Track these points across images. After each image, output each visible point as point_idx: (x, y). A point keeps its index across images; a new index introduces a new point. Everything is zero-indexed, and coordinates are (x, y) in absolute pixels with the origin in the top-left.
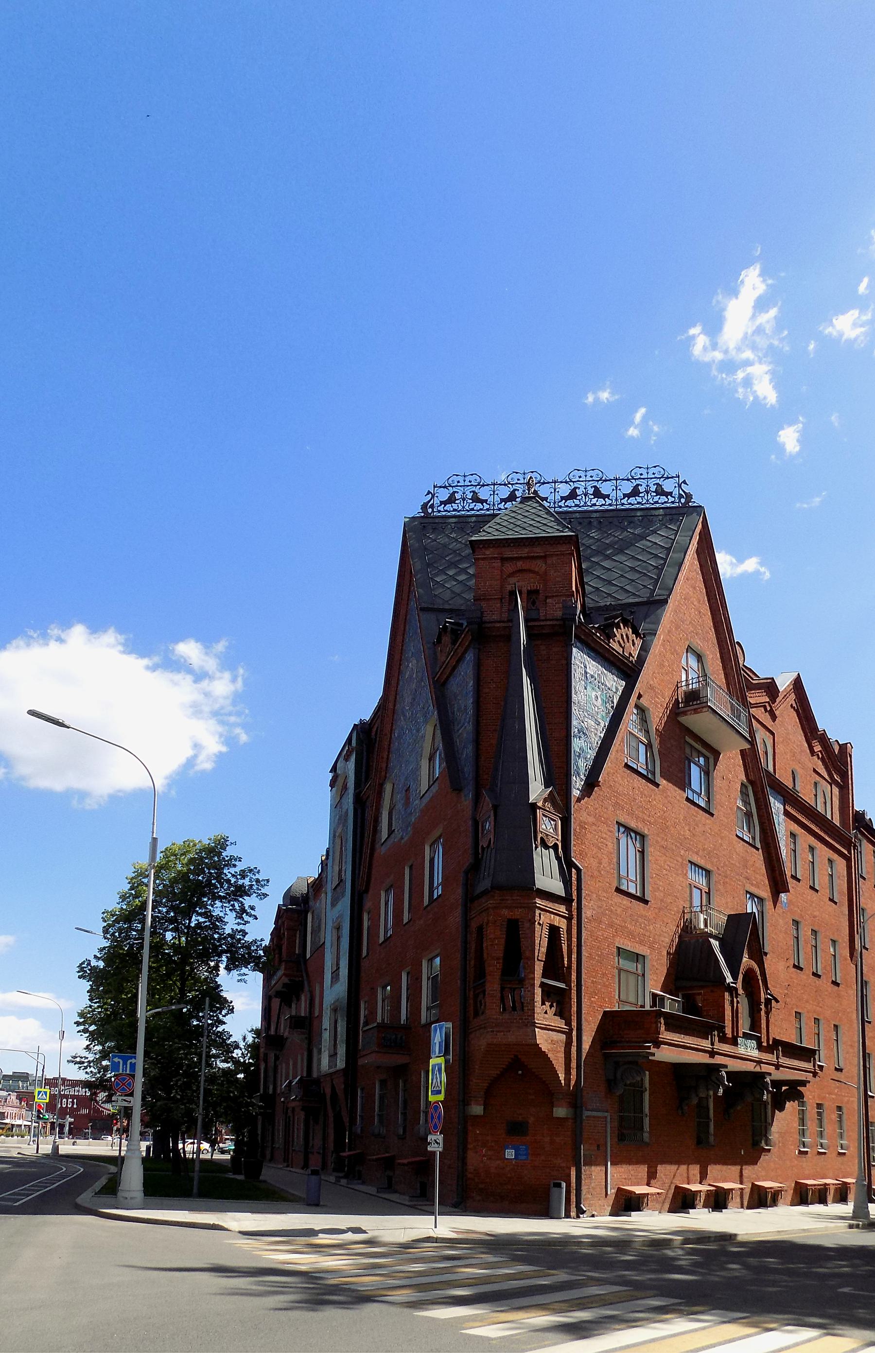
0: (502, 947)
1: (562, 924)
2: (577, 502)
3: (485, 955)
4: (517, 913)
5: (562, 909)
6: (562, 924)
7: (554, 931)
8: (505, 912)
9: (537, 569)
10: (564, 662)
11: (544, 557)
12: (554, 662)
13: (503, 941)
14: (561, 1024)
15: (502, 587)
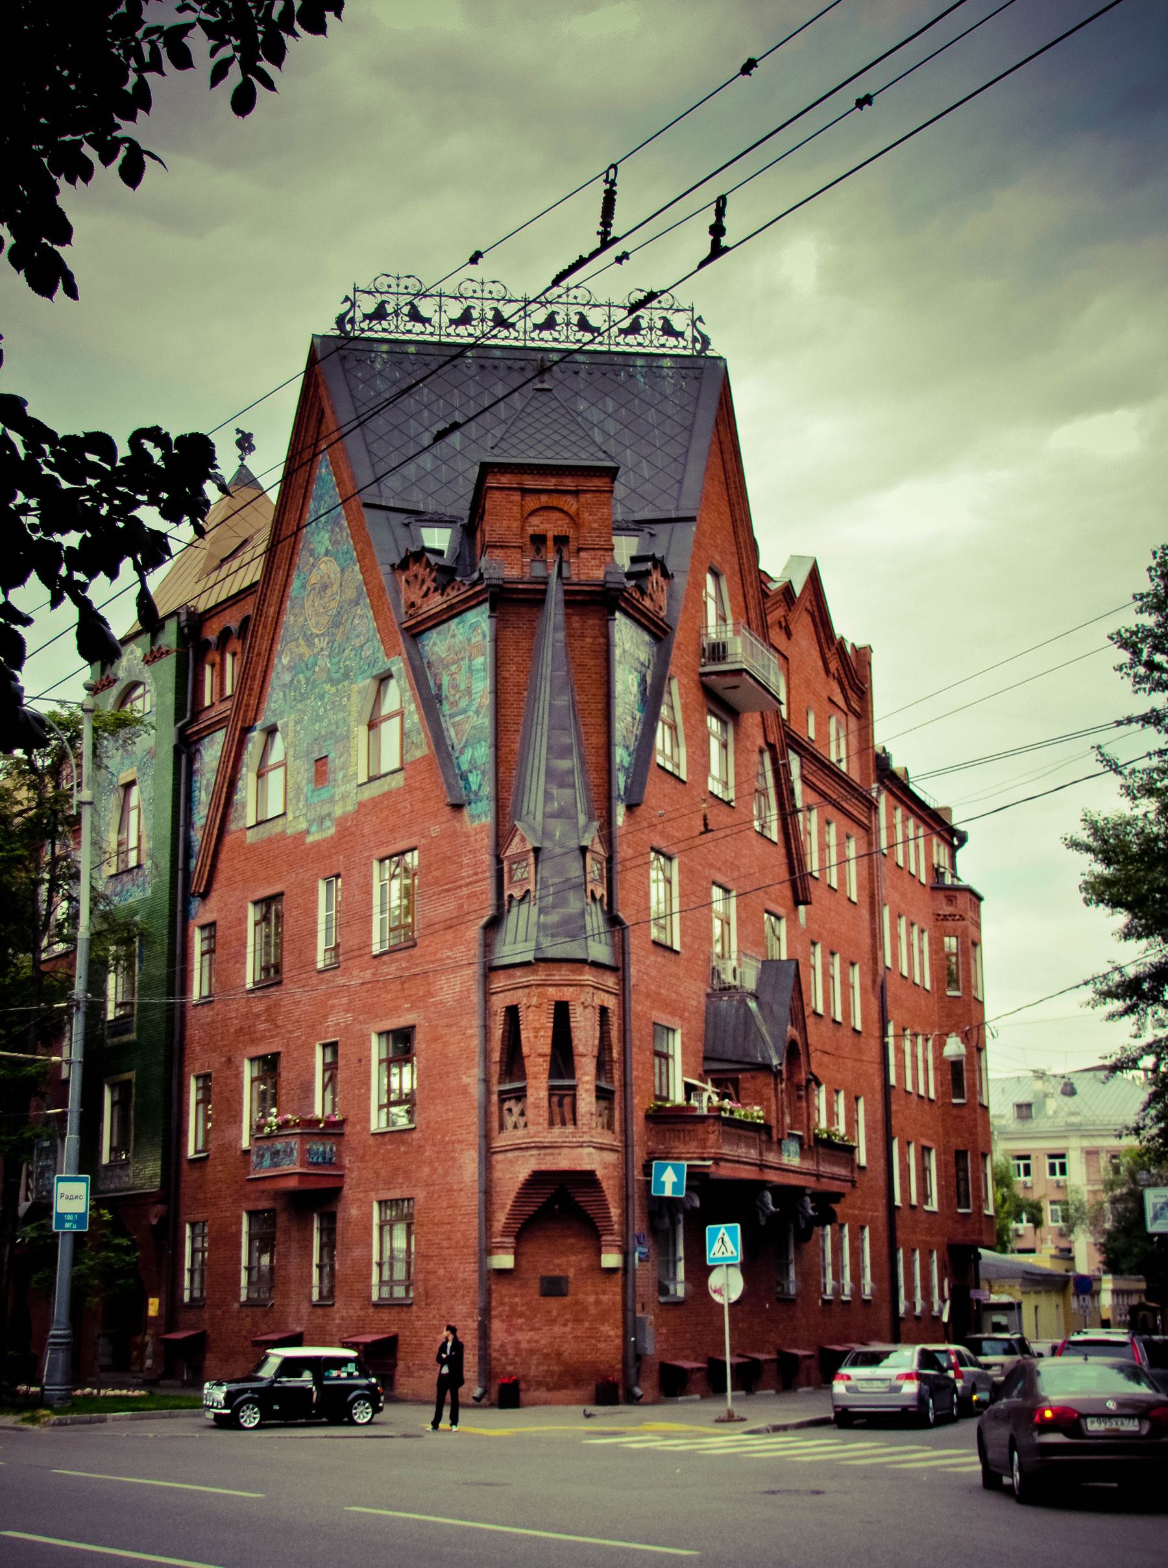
0: (549, 1041)
1: (611, 1002)
2: (556, 335)
3: (525, 1050)
4: (567, 994)
5: (610, 981)
6: (611, 1002)
7: (604, 1011)
8: (551, 991)
9: (566, 508)
10: (602, 640)
11: (576, 493)
12: (589, 640)
13: (550, 1033)
14: (607, 1139)
15: (523, 528)
